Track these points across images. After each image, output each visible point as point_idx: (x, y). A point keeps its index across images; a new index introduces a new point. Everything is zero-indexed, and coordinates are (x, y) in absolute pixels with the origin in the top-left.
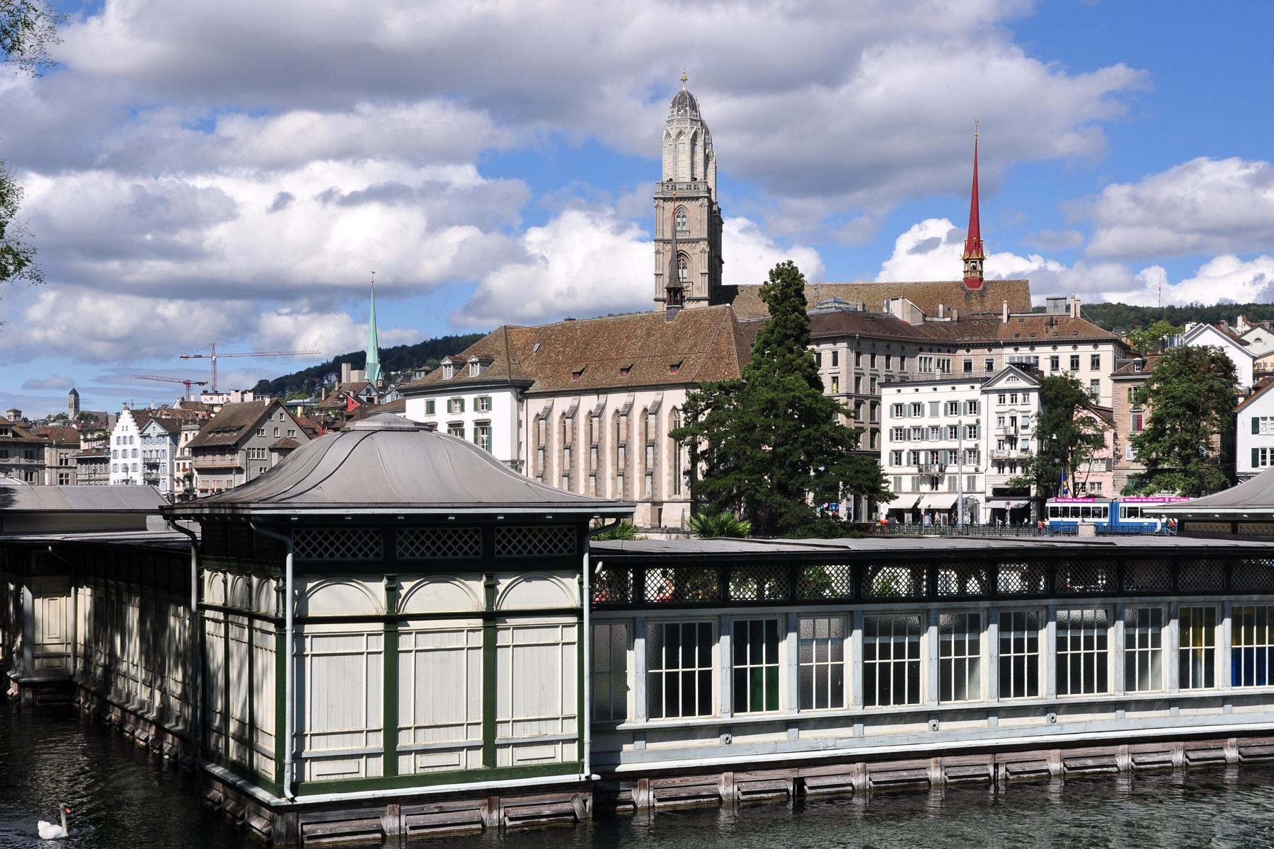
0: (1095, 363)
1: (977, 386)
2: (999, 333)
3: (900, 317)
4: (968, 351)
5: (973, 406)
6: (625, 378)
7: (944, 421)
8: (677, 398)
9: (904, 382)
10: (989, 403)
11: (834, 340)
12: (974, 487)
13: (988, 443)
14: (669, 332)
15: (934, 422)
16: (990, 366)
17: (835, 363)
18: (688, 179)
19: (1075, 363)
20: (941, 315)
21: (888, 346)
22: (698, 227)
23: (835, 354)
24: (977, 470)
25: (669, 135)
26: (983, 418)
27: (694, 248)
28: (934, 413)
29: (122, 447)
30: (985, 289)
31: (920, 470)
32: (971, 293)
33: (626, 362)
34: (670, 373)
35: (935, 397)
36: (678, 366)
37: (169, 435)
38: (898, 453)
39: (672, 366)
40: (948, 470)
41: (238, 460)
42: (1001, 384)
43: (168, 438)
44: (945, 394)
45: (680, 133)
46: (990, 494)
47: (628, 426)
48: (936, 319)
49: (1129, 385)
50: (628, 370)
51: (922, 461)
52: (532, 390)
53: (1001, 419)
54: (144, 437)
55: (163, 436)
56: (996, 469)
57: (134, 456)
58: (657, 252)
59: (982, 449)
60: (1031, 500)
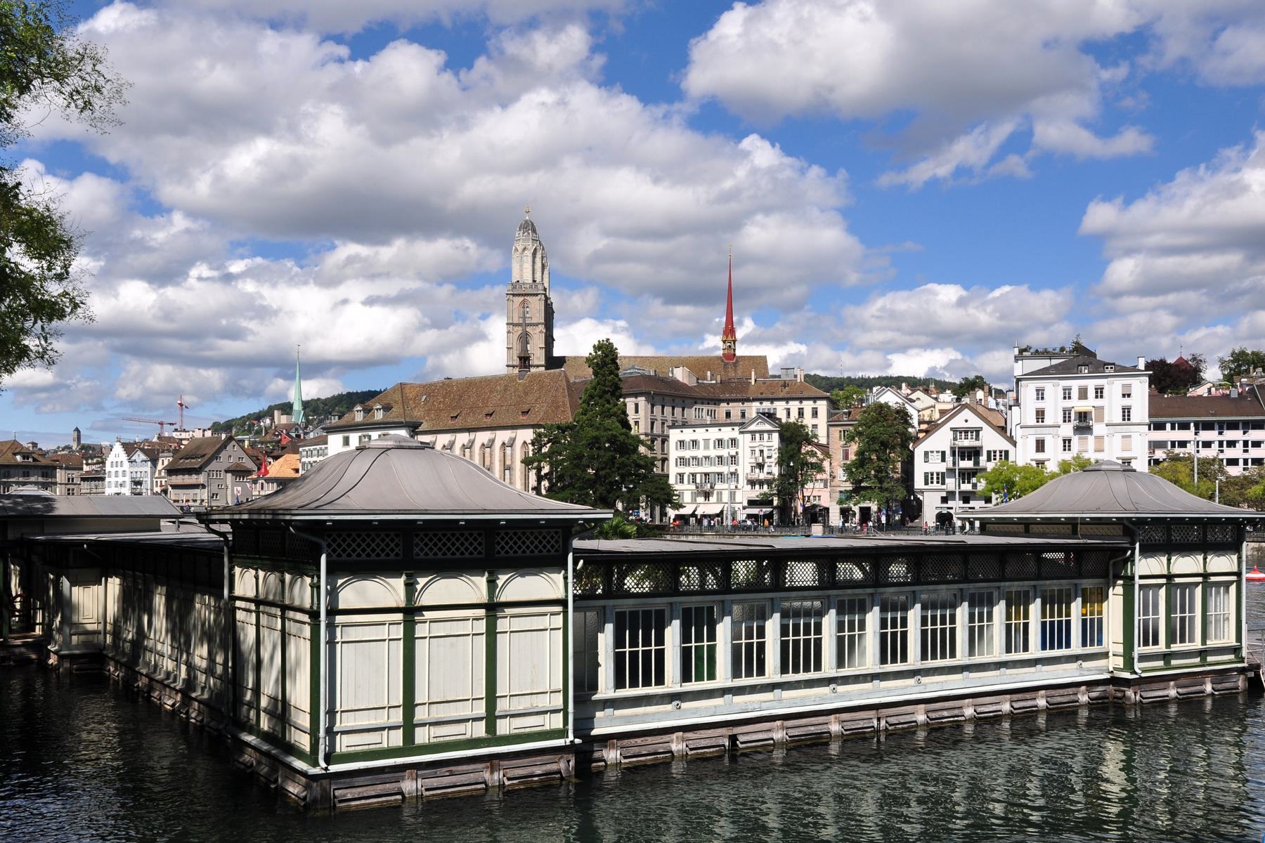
0: (815, 413)
1: (737, 428)
2: (749, 392)
3: (681, 380)
4: (728, 404)
5: (734, 442)
6: (489, 421)
7: (713, 453)
8: (527, 435)
9: (685, 425)
10: (745, 440)
11: (636, 395)
12: (734, 499)
13: (744, 468)
14: (520, 388)
15: (707, 453)
16: (743, 415)
17: (637, 411)
18: (531, 282)
19: (801, 413)
20: (709, 379)
21: (673, 400)
22: (538, 315)
23: (637, 405)
24: (736, 487)
25: (516, 250)
26: (740, 450)
27: (535, 330)
28: (707, 447)
29: (115, 469)
30: (737, 361)
31: (697, 487)
32: (727, 364)
33: (487, 410)
34: (521, 418)
35: (707, 436)
36: (527, 412)
37: (150, 460)
38: (681, 475)
39: (523, 412)
40: (716, 487)
41: (201, 479)
42: (753, 427)
43: (149, 463)
44: (714, 433)
45: (525, 249)
46: (745, 504)
47: (491, 455)
48: (705, 382)
49: (840, 428)
50: (491, 415)
51: (698, 481)
52: (421, 429)
53: (753, 452)
54: (132, 462)
55: (145, 461)
56: (750, 486)
57: (124, 475)
58: (509, 332)
59: (740, 472)
60: (775, 508)
